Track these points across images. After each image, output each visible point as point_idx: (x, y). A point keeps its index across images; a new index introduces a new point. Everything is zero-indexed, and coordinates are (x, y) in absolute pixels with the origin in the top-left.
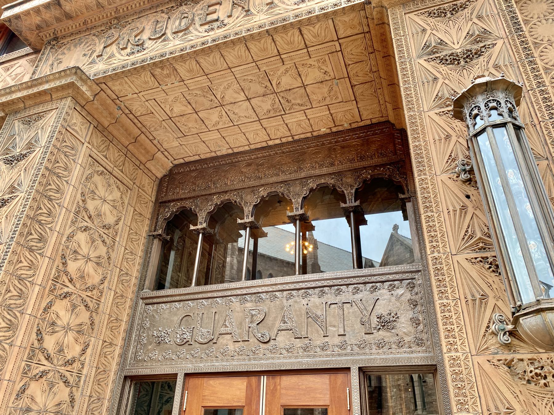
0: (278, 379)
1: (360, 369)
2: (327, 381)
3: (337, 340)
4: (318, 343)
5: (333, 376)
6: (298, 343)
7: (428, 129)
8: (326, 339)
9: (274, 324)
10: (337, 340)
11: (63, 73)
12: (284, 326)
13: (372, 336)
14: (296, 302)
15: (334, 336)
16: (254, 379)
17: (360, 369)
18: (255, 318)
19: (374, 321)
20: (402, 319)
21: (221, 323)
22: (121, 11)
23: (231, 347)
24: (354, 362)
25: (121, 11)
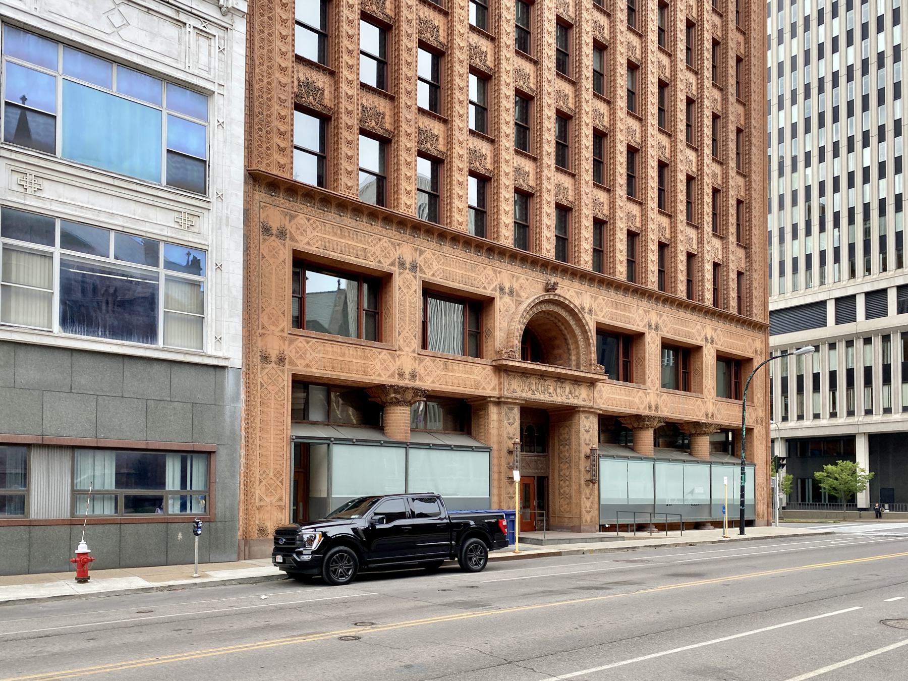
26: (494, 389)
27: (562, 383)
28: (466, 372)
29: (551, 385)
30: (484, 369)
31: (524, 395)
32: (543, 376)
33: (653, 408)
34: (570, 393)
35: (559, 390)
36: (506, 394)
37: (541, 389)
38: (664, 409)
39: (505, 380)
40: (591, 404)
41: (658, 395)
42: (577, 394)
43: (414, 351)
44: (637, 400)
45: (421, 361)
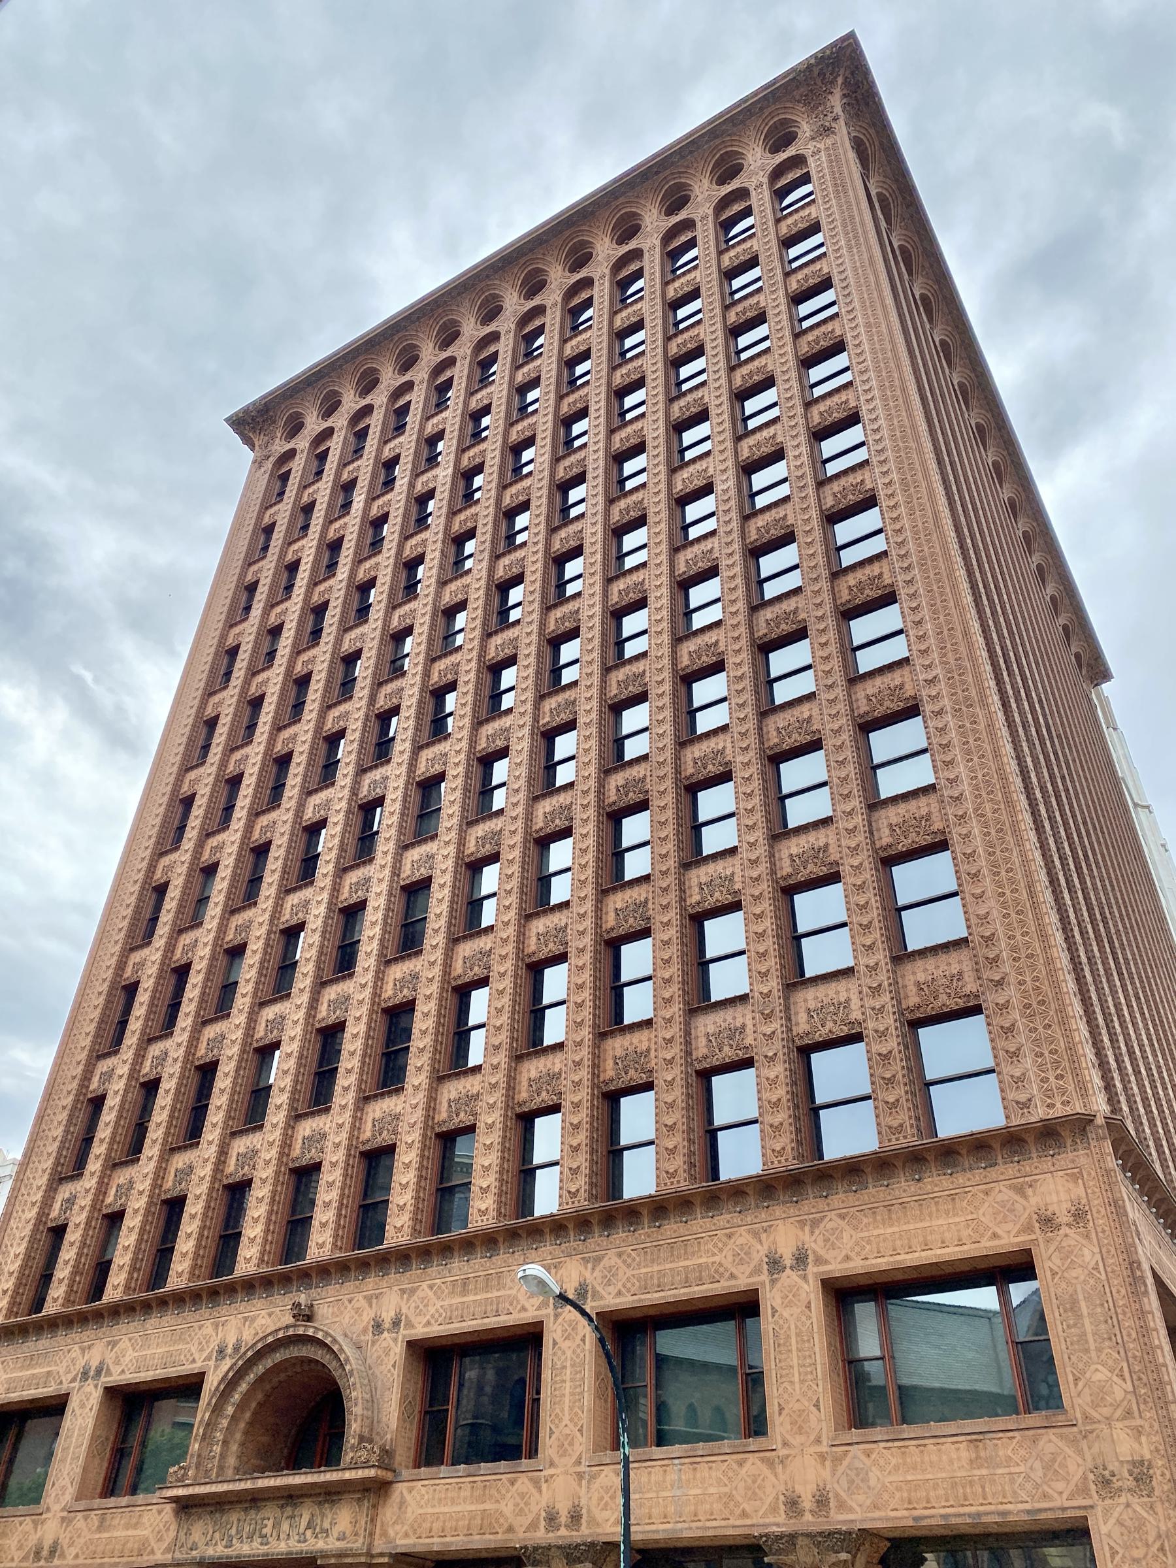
27: (295, 1506)
28: (127, 1527)
29: (270, 1513)
30: (159, 1512)
31: (210, 1552)
32: (290, 1497)
33: (45, 1553)
35: (285, 1526)
36: (178, 1555)
38: (600, 1516)
40: (358, 1544)
41: (580, 1476)
42: (326, 1525)
43: (63, 1510)
44: (507, 1508)
45: (70, 1521)
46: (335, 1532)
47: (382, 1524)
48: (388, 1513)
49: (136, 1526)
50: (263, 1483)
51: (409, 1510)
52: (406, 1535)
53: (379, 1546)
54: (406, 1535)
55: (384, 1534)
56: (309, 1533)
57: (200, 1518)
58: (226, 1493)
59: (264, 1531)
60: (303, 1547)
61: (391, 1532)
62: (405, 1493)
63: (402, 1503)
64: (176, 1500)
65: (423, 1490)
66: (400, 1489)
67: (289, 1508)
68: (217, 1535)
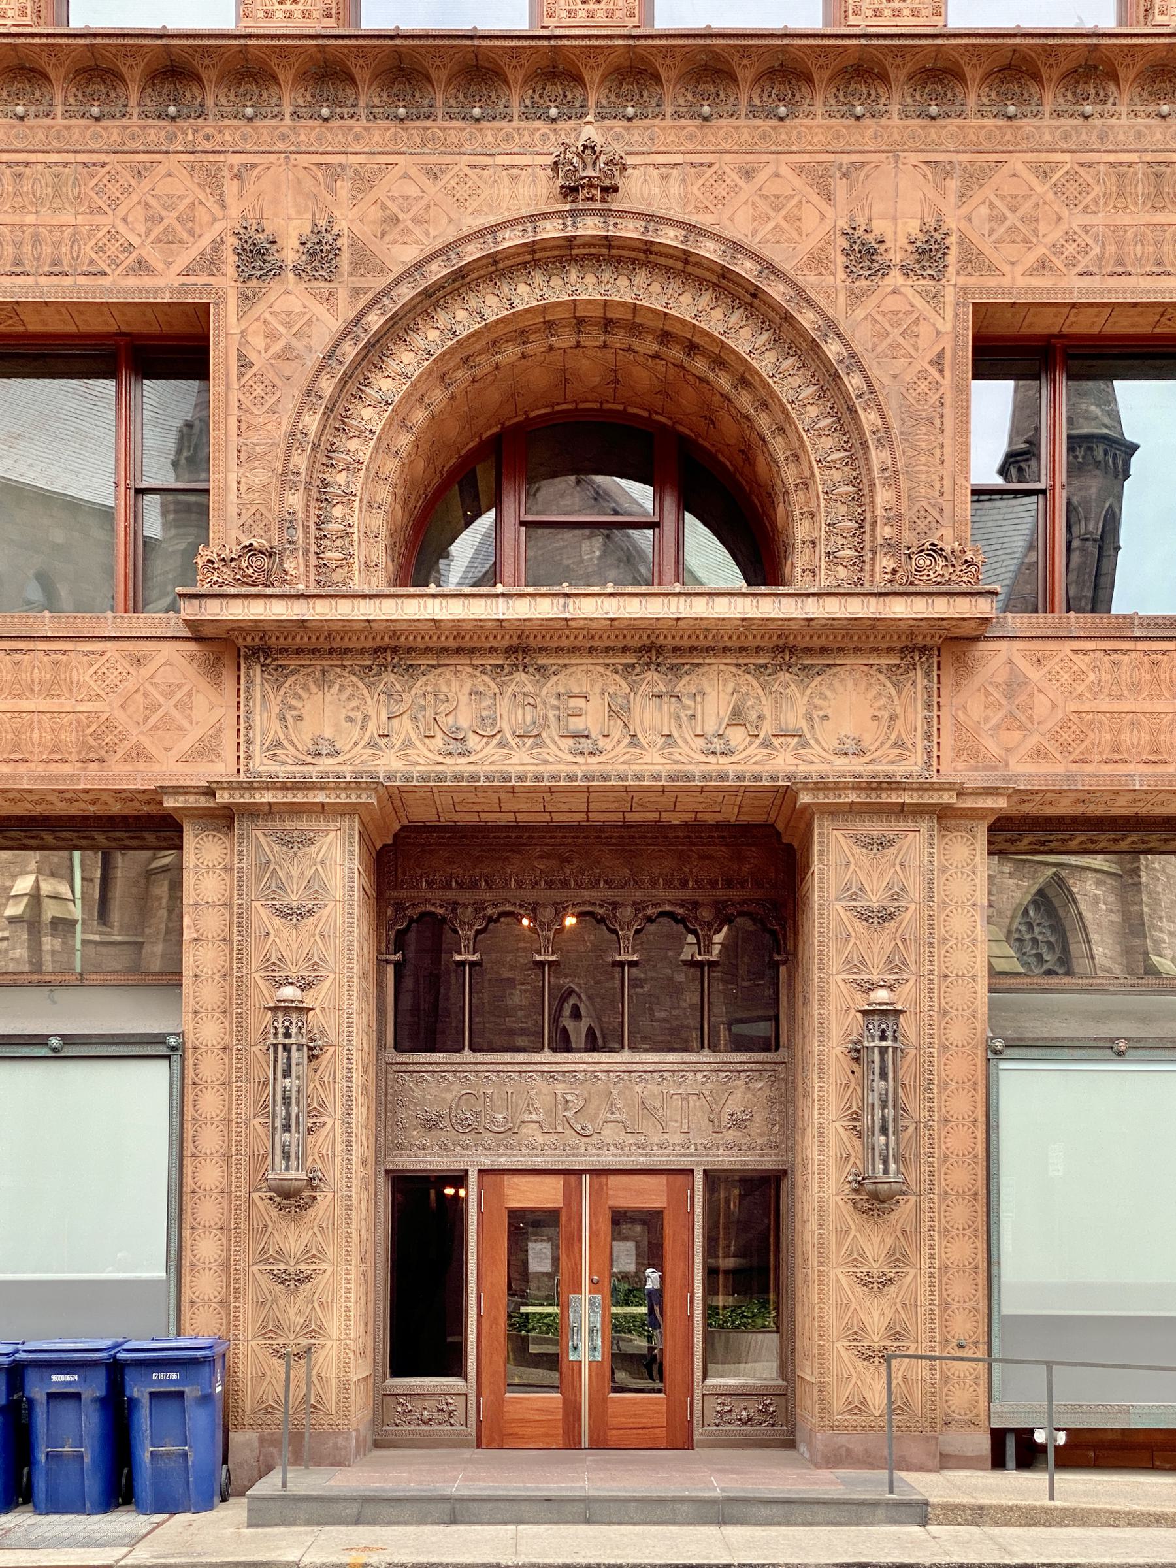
0: (603, 1179)
1: (705, 1171)
2: (665, 1182)
3: (679, 1139)
4: (657, 1140)
5: (671, 1177)
6: (630, 1139)
7: (833, 999)
8: (666, 1136)
9: (596, 1115)
10: (679, 1139)
11: (353, 785)
12: (612, 1117)
13: (720, 1135)
14: (626, 1088)
15: (675, 1133)
16: (573, 1179)
17: (705, 1171)
18: (571, 1105)
19: (725, 1118)
20: (757, 1118)
21: (522, 1105)
22: (403, 638)
23: (540, 1139)
24: (699, 1164)
25: (403, 638)
26: (206, 750)
31: (390, 763)
34: (737, 718)
37: (513, 716)
39: (265, 701)
40: (912, 766)
42: (793, 718)
46: (827, 736)
47: (959, 726)
48: (974, 701)
49: (49, 690)
50: (589, 609)
51: (1040, 699)
52: (1038, 754)
53: (955, 770)
54: (1038, 754)
55: (970, 750)
56: (737, 736)
57: (323, 682)
58: (479, 625)
59: (577, 724)
60: (730, 766)
61: (991, 745)
62: (1023, 664)
63: (1014, 686)
64: (199, 633)
65: (1081, 662)
66: (995, 659)
67: (651, 675)
68: (405, 726)
